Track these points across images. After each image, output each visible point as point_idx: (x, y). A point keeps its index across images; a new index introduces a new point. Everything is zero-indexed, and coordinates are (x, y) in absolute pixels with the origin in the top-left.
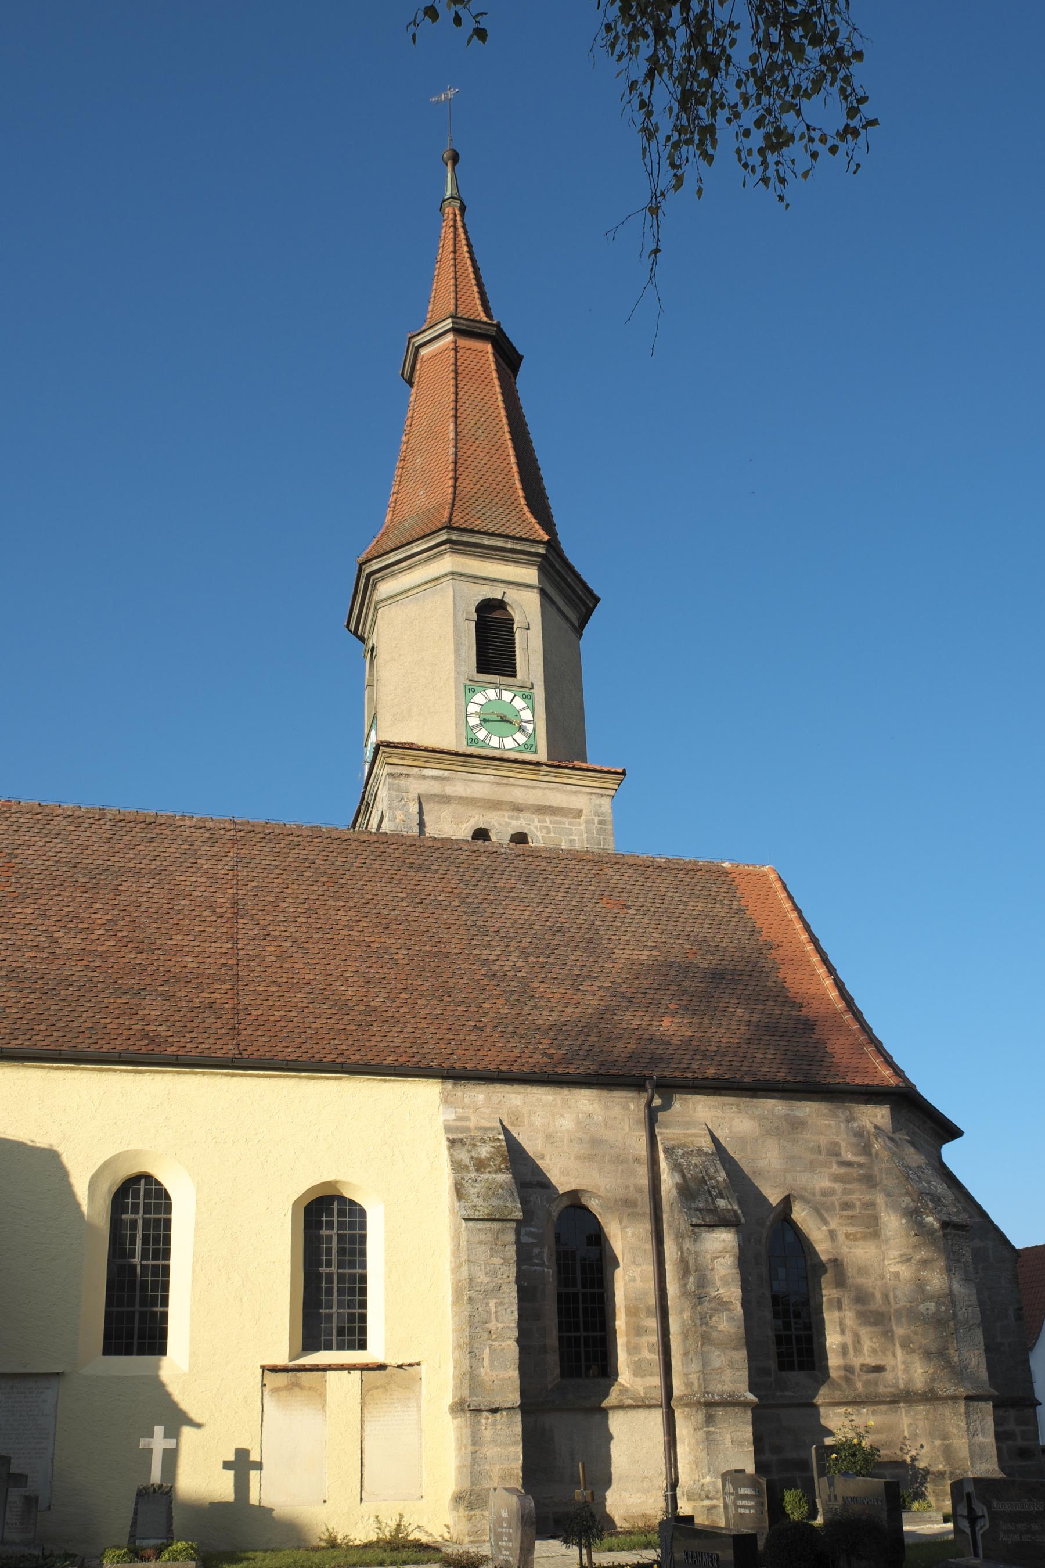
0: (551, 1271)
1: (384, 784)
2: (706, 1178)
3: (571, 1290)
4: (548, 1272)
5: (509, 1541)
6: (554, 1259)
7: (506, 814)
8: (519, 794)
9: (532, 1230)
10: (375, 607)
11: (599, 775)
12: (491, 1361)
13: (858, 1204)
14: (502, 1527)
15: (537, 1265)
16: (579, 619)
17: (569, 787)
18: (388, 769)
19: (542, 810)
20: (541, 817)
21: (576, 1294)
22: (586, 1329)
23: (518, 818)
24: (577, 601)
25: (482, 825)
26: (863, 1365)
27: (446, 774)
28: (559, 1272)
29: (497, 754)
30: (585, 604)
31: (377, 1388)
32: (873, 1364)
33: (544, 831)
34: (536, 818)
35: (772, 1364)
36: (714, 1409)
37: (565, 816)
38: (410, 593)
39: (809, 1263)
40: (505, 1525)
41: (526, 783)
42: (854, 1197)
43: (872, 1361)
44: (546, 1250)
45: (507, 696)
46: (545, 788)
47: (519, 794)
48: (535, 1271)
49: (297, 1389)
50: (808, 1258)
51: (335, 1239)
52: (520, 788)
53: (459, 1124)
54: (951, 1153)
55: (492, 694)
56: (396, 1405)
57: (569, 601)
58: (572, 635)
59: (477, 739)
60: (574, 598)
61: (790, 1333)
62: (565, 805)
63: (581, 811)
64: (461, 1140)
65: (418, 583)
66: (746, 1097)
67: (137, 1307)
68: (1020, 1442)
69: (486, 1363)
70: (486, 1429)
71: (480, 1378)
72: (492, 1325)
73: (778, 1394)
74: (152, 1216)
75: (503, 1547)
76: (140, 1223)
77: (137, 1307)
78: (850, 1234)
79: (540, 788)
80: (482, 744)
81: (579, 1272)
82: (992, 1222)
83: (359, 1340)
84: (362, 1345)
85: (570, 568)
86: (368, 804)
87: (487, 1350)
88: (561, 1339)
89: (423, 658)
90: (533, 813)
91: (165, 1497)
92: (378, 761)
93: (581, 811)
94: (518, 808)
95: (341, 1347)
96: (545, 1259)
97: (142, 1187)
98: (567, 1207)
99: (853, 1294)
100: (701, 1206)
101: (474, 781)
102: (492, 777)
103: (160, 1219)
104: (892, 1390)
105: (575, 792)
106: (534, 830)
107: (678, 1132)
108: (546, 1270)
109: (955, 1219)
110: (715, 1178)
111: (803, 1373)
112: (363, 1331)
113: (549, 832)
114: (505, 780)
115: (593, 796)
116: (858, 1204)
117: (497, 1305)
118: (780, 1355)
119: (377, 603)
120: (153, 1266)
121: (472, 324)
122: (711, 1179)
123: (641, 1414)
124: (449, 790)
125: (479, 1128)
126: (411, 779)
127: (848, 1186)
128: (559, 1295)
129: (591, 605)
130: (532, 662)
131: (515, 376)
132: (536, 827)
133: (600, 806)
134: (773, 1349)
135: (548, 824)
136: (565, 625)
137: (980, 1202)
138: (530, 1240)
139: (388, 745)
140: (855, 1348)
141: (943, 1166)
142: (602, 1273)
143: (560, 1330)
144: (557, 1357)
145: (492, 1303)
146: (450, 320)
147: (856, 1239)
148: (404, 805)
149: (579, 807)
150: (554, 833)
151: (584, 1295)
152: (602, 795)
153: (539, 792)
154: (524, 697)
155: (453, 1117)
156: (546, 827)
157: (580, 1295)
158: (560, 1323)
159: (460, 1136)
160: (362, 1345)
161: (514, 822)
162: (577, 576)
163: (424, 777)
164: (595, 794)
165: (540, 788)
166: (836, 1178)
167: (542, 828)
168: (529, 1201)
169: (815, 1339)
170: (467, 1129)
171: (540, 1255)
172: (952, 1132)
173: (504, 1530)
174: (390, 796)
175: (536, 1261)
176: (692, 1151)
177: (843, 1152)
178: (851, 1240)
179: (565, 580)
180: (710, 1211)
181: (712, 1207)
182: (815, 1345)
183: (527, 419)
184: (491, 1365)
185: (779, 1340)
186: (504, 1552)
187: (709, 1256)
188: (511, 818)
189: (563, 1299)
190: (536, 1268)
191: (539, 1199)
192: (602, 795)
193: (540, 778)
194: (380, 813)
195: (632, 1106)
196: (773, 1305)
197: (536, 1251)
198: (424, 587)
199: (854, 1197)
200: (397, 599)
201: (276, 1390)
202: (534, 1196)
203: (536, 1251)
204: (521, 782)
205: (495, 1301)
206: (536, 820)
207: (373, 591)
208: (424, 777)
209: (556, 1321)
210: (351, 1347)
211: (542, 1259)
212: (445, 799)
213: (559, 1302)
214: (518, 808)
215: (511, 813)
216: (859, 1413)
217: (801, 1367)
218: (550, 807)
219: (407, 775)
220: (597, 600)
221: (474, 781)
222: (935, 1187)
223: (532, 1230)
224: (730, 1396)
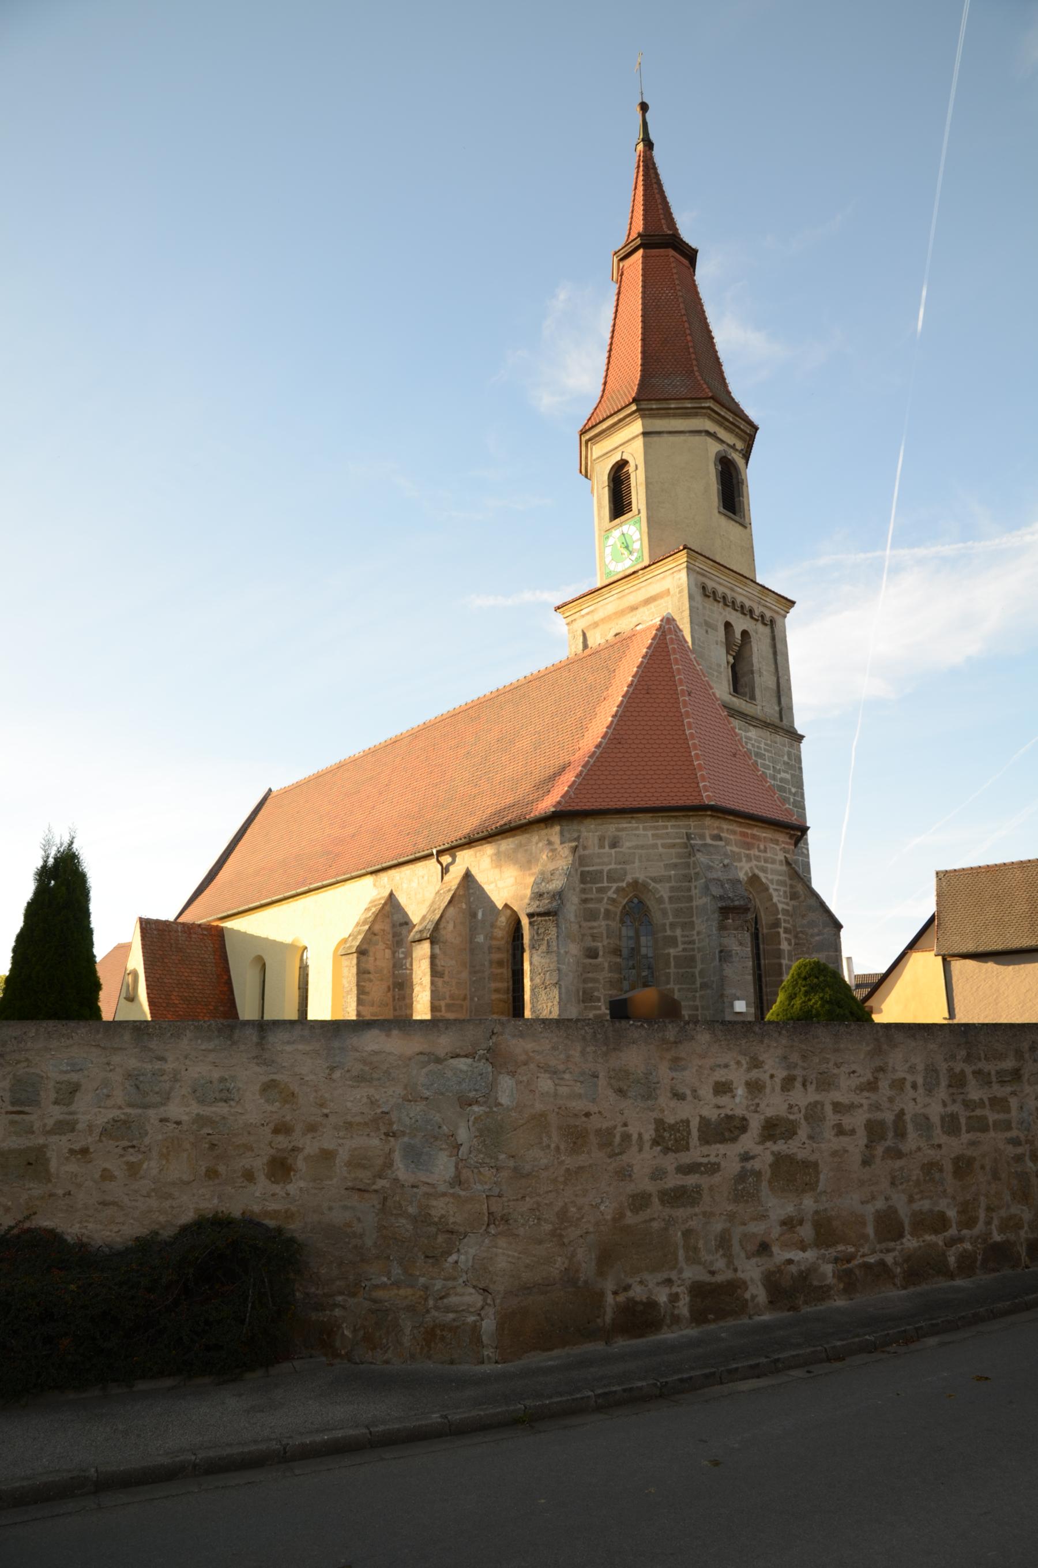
17: (659, 577)
27: (592, 608)
41: (635, 588)
46: (646, 586)
63: (669, 590)
66: (485, 844)
79: (642, 587)
90: (644, 606)
93: (669, 590)
94: (634, 608)
101: (607, 604)
115: (675, 574)
124: (597, 617)
126: (578, 621)
130: (639, 494)
133: (680, 579)
149: (667, 588)
152: (680, 570)
153: (643, 590)
163: (583, 616)
165: (642, 587)
188: (632, 617)
192: (680, 570)
208: (583, 616)
212: (596, 625)
214: (634, 608)
215: (632, 614)
218: (651, 597)
219: (575, 620)
221: (607, 604)
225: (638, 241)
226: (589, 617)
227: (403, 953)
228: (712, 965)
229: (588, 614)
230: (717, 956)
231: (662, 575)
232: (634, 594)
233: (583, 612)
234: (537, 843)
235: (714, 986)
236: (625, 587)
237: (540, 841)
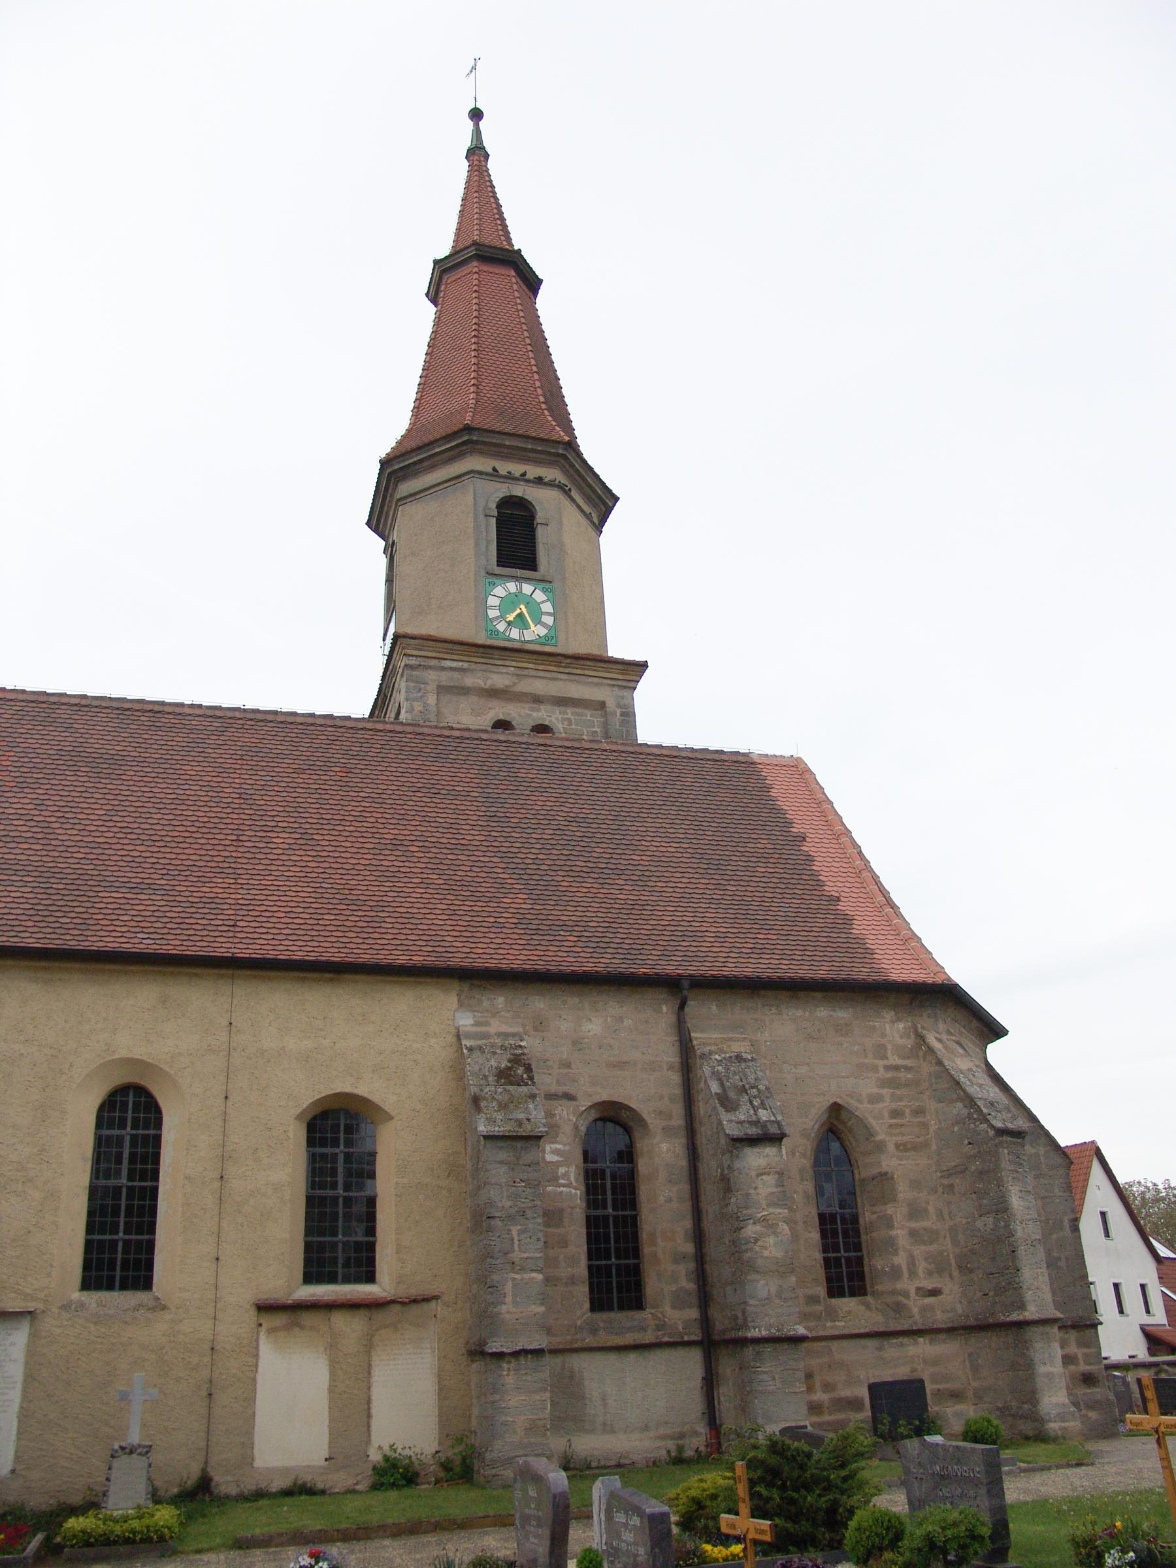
0: (578, 1192)
1: (402, 675)
2: (747, 1087)
3: (600, 1212)
4: (576, 1194)
5: (539, 1526)
6: (582, 1179)
7: (527, 706)
8: (538, 686)
9: (558, 1146)
10: (396, 504)
11: (620, 667)
12: (515, 1295)
13: (907, 1111)
14: (530, 1508)
15: (563, 1186)
16: (599, 517)
17: (590, 679)
18: (406, 661)
19: (562, 702)
20: (563, 709)
21: (606, 1218)
22: (617, 1258)
23: (539, 710)
24: (597, 500)
25: (501, 717)
26: (918, 1289)
27: (466, 665)
28: (588, 1192)
29: (517, 645)
30: (605, 503)
31: (386, 1327)
32: (929, 1288)
33: (566, 723)
34: (557, 710)
35: (821, 1291)
36: (761, 1345)
37: (586, 707)
38: (431, 491)
39: (857, 1177)
40: (533, 1506)
42: (903, 1104)
43: (929, 1285)
44: (573, 1169)
45: (527, 588)
47: (538, 686)
48: (562, 1192)
49: (297, 1329)
50: (856, 1172)
51: (341, 1158)
52: (541, 680)
53: (479, 1029)
54: (996, 1052)
55: (512, 586)
56: (408, 1346)
57: (589, 500)
58: (591, 532)
59: (498, 631)
60: (594, 497)
61: (839, 1255)
62: (587, 696)
64: (480, 1048)
65: (439, 481)
67: (121, 1234)
68: (1083, 1367)
69: (509, 1299)
70: (508, 1375)
71: (501, 1316)
72: (517, 1255)
73: (829, 1324)
74: (141, 1132)
75: (531, 1532)
76: (127, 1139)
77: (121, 1234)
78: (901, 1144)
80: (500, 636)
81: (609, 1192)
82: (1042, 1127)
83: (367, 1272)
84: (370, 1278)
85: (591, 469)
86: (386, 696)
87: (510, 1284)
88: (590, 1267)
89: (443, 553)
91: (144, 1458)
92: (396, 652)
94: (537, 700)
95: (347, 1280)
96: (573, 1180)
97: (131, 1099)
98: (596, 1120)
99: (905, 1210)
100: (742, 1117)
102: (513, 669)
103: (148, 1135)
104: (951, 1315)
105: (597, 684)
106: (555, 722)
107: (715, 1036)
108: (573, 1191)
109: (1010, 1126)
110: (756, 1087)
111: (854, 1299)
112: (371, 1262)
113: (570, 723)
114: (526, 672)
115: (616, 689)
116: (907, 1111)
117: (520, 1233)
118: (829, 1280)
119: (399, 500)
120: (141, 1188)
121: (491, 251)
122: (752, 1087)
123: (681, 1352)
124: (469, 681)
125: (499, 1034)
127: (898, 1092)
128: (588, 1218)
129: (611, 504)
131: (535, 297)
132: (557, 719)
134: (821, 1273)
135: (569, 716)
136: (584, 522)
137: (1029, 1106)
138: (555, 1158)
139: (405, 636)
140: (909, 1270)
141: (990, 1068)
142: (634, 1194)
143: (590, 1258)
144: (586, 1289)
145: (514, 1231)
146: (473, 248)
147: (906, 1150)
148: (421, 697)
150: (576, 725)
151: (616, 1217)
153: (561, 684)
154: (544, 591)
155: (471, 1021)
156: (569, 720)
157: (611, 1219)
158: (589, 1250)
159: (479, 1042)
160: (370, 1278)
161: (535, 714)
162: (597, 476)
163: (443, 669)
164: (618, 686)
166: (884, 1083)
167: (563, 720)
168: (554, 1115)
169: (866, 1261)
170: (486, 1036)
171: (566, 1175)
172: (993, 1030)
173: (532, 1512)
174: (407, 688)
175: (562, 1181)
176: (731, 1057)
177: (889, 1054)
178: (901, 1151)
179: (584, 480)
180: (751, 1123)
181: (754, 1118)
182: (866, 1269)
183: (546, 335)
184: (514, 1302)
185: (827, 1262)
186: (532, 1540)
187: (753, 1173)
188: (532, 709)
189: (592, 1223)
190: (562, 1189)
191: (565, 1112)
193: (561, 670)
194: (397, 705)
195: (664, 1009)
196: (820, 1225)
197: (562, 1170)
198: (446, 485)
199: (903, 1104)
200: (418, 497)
201: (272, 1331)
202: (560, 1108)
203: (562, 1170)
204: (541, 674)
205: (519, 1227)
206: (558, 712)
207: (394, 489)
208: (443, 669)
209: (585, 1247)
210: (358, 1280)
211: (568, 1179)
213: (588, 1227)
214: (537, 700)
216: (916, 1343)
217: (853, 1294)
220: (616, 499)
222: (988, 1091)
223: (558, 1146)
224: (778, 1330)
225: (472, 251)
226: (456, 675)
227: (556, 1152)
228: (1054, 1236)
229: (451, 669)
230: (1066, 1223)
231: (596, 680)
232: (545, 681)
233: (448, 664)
234: (893, 1022)
235: (1062, 1264)
236: (531, 666)
237: (899, 1020)
